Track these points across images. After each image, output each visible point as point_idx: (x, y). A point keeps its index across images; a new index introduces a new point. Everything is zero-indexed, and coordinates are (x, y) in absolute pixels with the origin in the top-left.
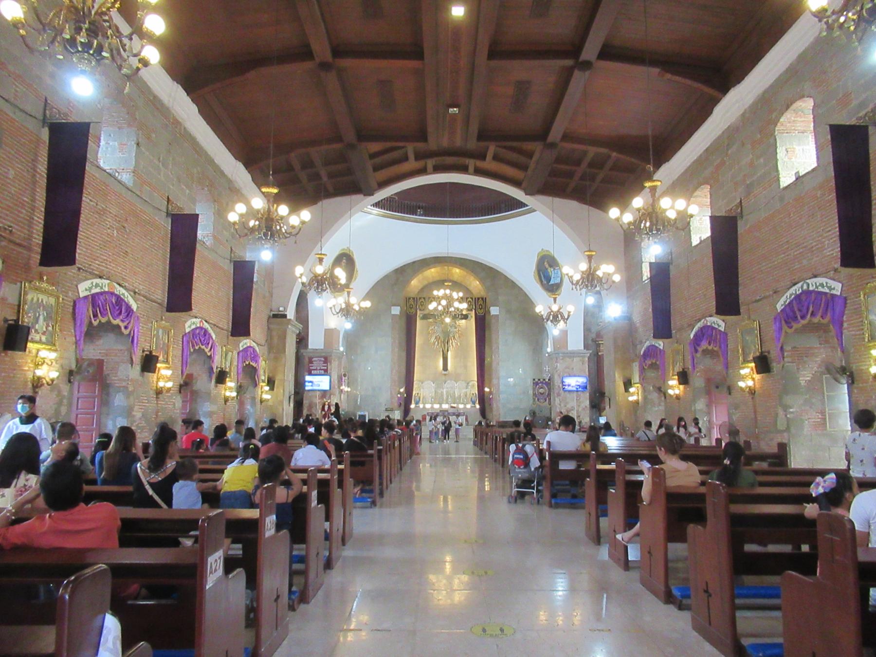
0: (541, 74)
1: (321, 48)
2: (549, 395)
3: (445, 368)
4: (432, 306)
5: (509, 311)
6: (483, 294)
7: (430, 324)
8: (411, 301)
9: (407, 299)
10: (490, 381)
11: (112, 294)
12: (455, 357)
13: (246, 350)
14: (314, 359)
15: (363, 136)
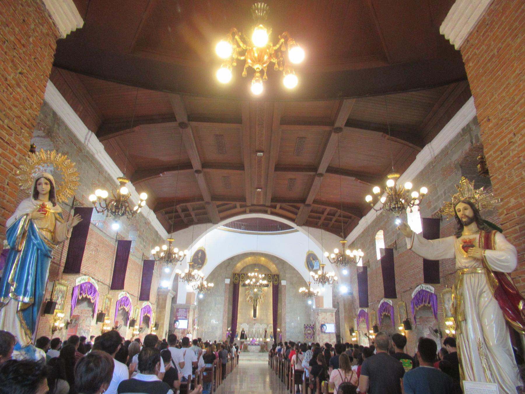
0: (300, 177)
1: (196, 164)
2: (314, 334)
3: (255, 315)
4: (247, 282)
5: (291, 283)
6: (277, 272)
7: (246, 290)
8: (237, 276)
9: (234, 275)
10: (281, 324)
11: (89, 283)
12: (261, 309)
13: (145, 308)
14: (180, 310)
15: (214, 198)
